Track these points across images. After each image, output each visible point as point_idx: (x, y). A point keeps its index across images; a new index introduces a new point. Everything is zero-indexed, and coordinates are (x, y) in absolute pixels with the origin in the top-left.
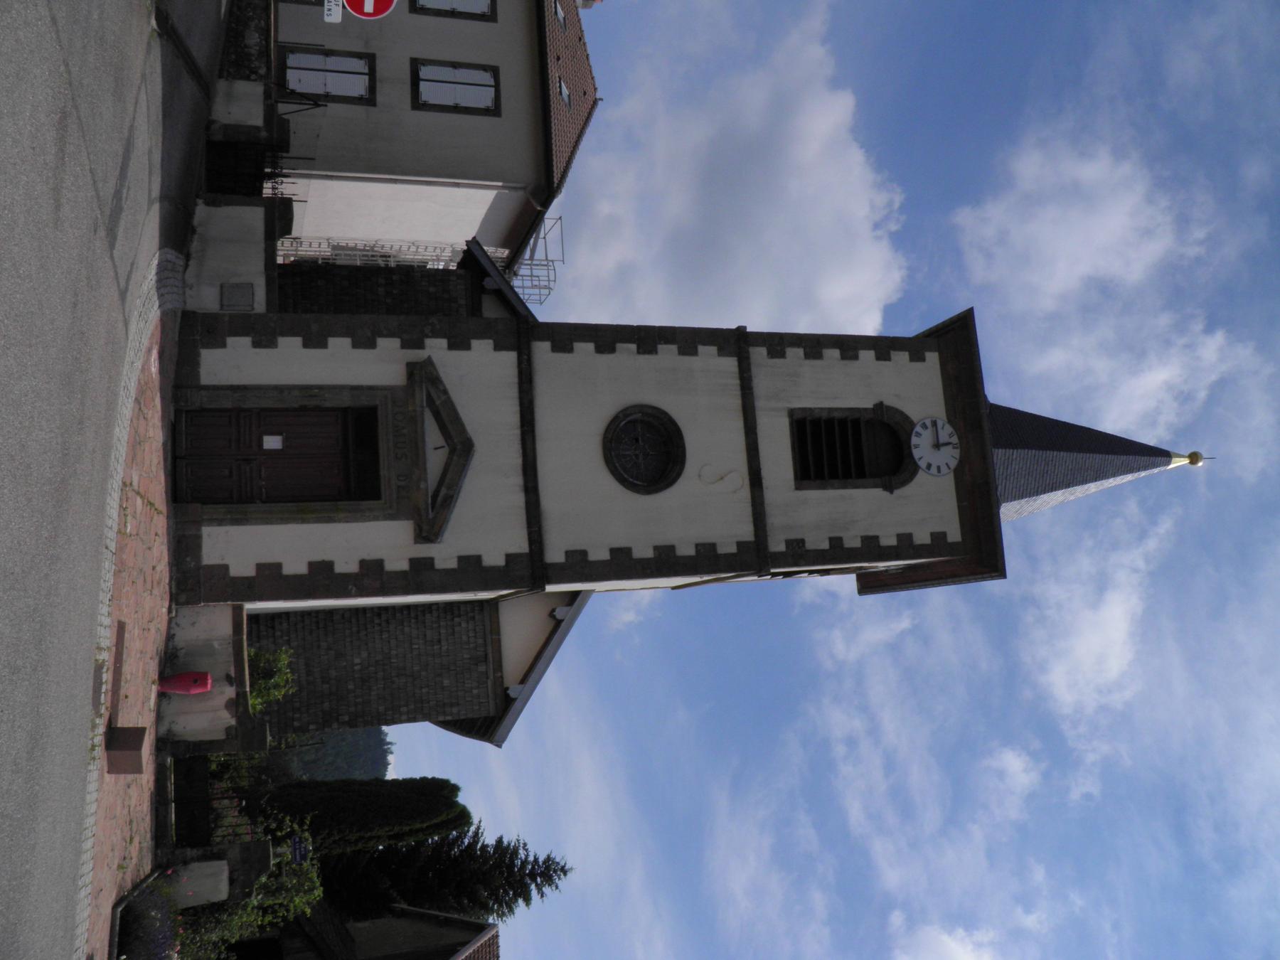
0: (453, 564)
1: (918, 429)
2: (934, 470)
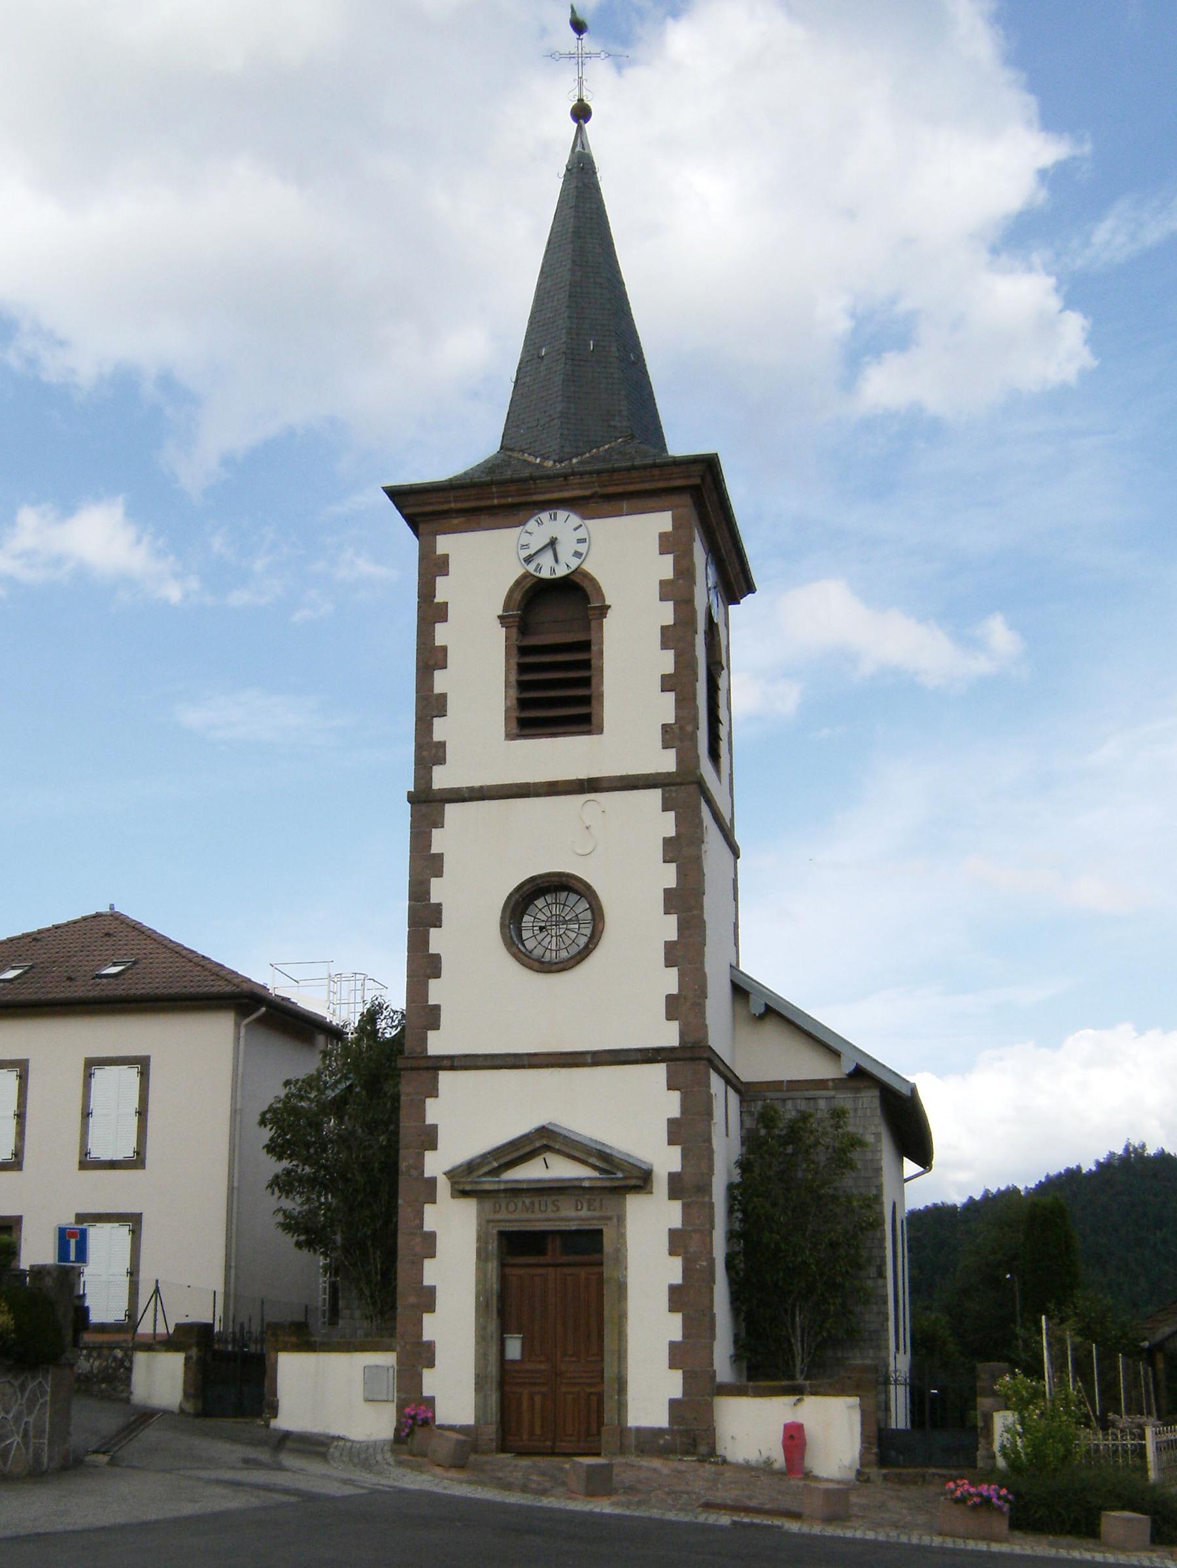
0: (676, 1151)
1: (531, 568)
2: (582, 548)
